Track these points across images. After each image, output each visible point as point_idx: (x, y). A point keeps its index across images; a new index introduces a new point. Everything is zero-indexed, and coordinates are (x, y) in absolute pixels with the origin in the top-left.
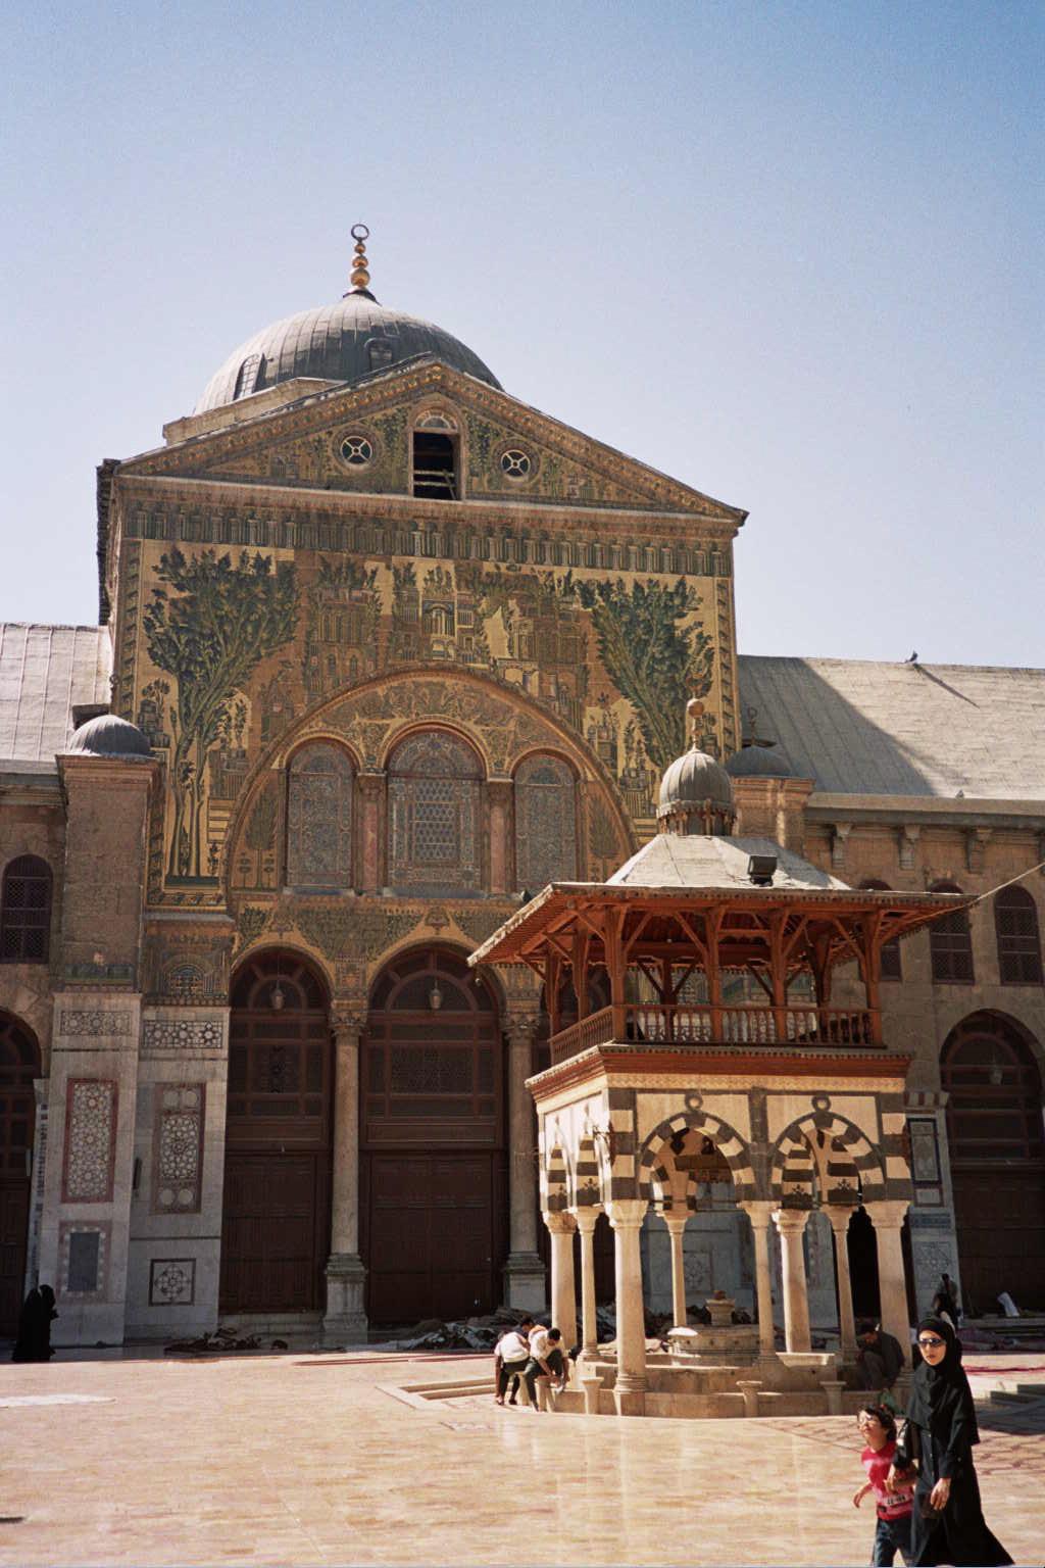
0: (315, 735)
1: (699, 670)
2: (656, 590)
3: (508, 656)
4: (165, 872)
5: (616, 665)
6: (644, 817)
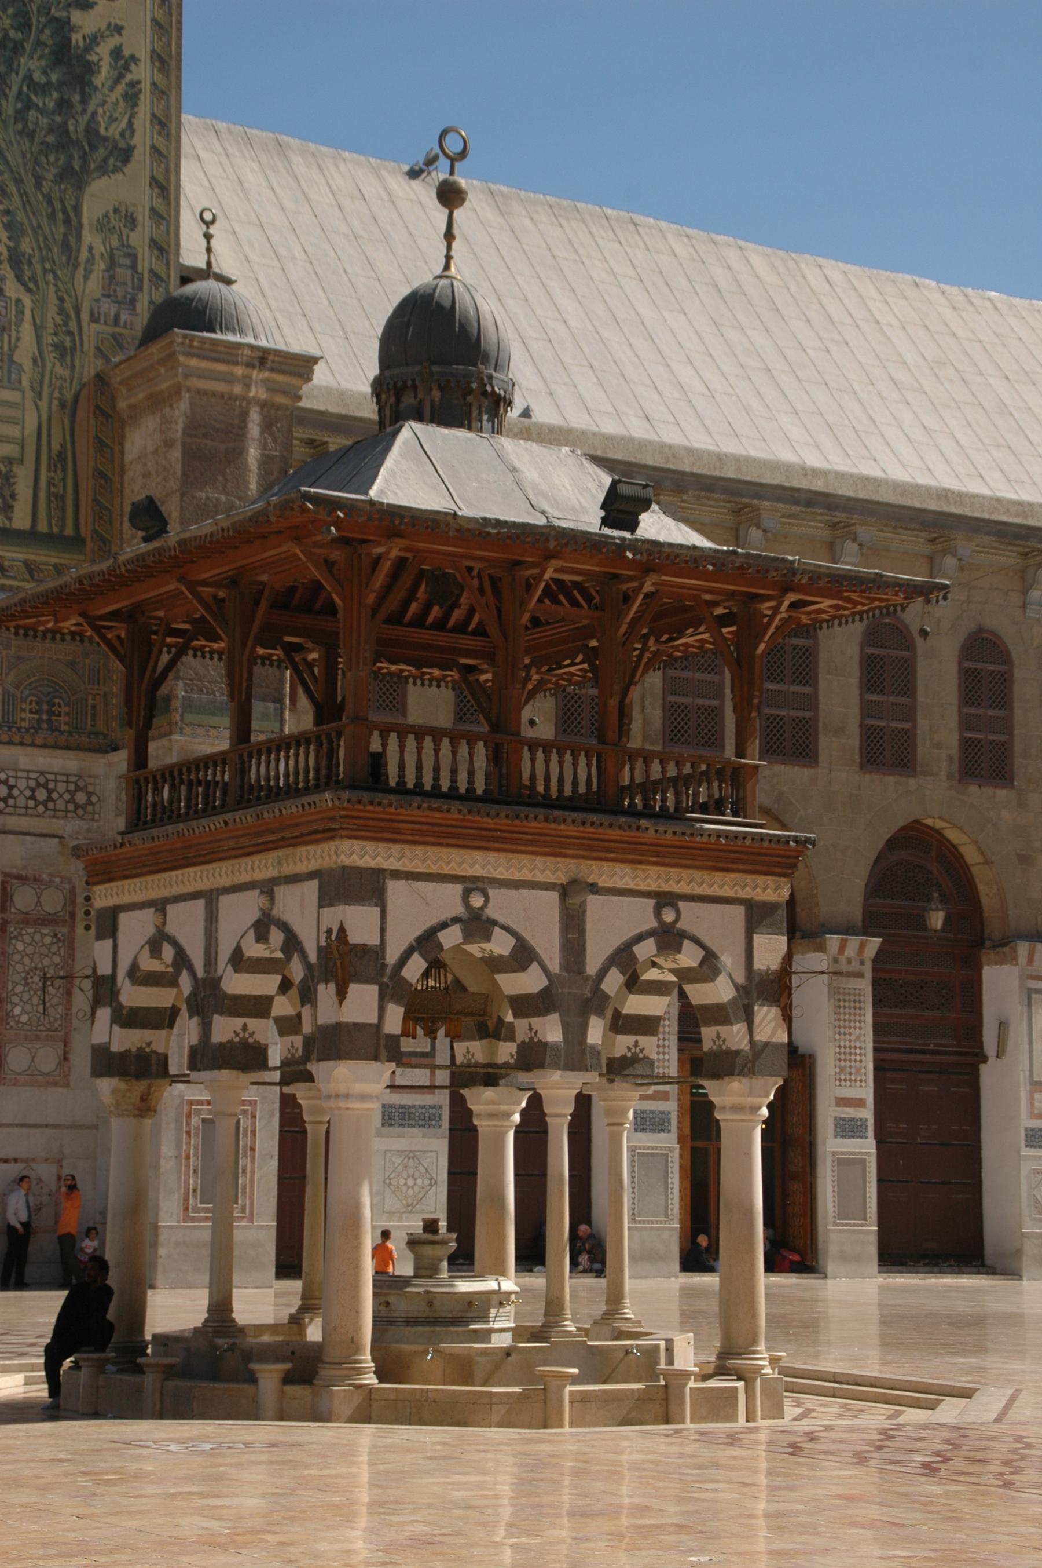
1: (112, 119)
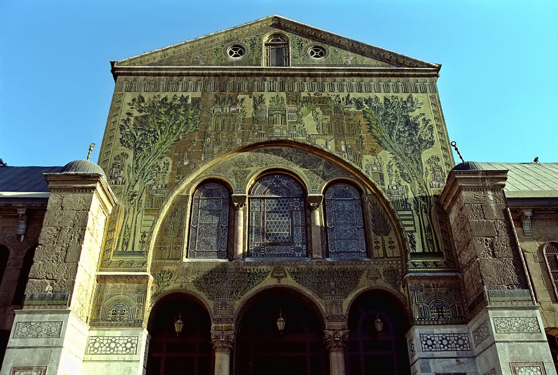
3: (317, 133)
4: (114, 248)
5: (378, 135)
6: (404, 210)
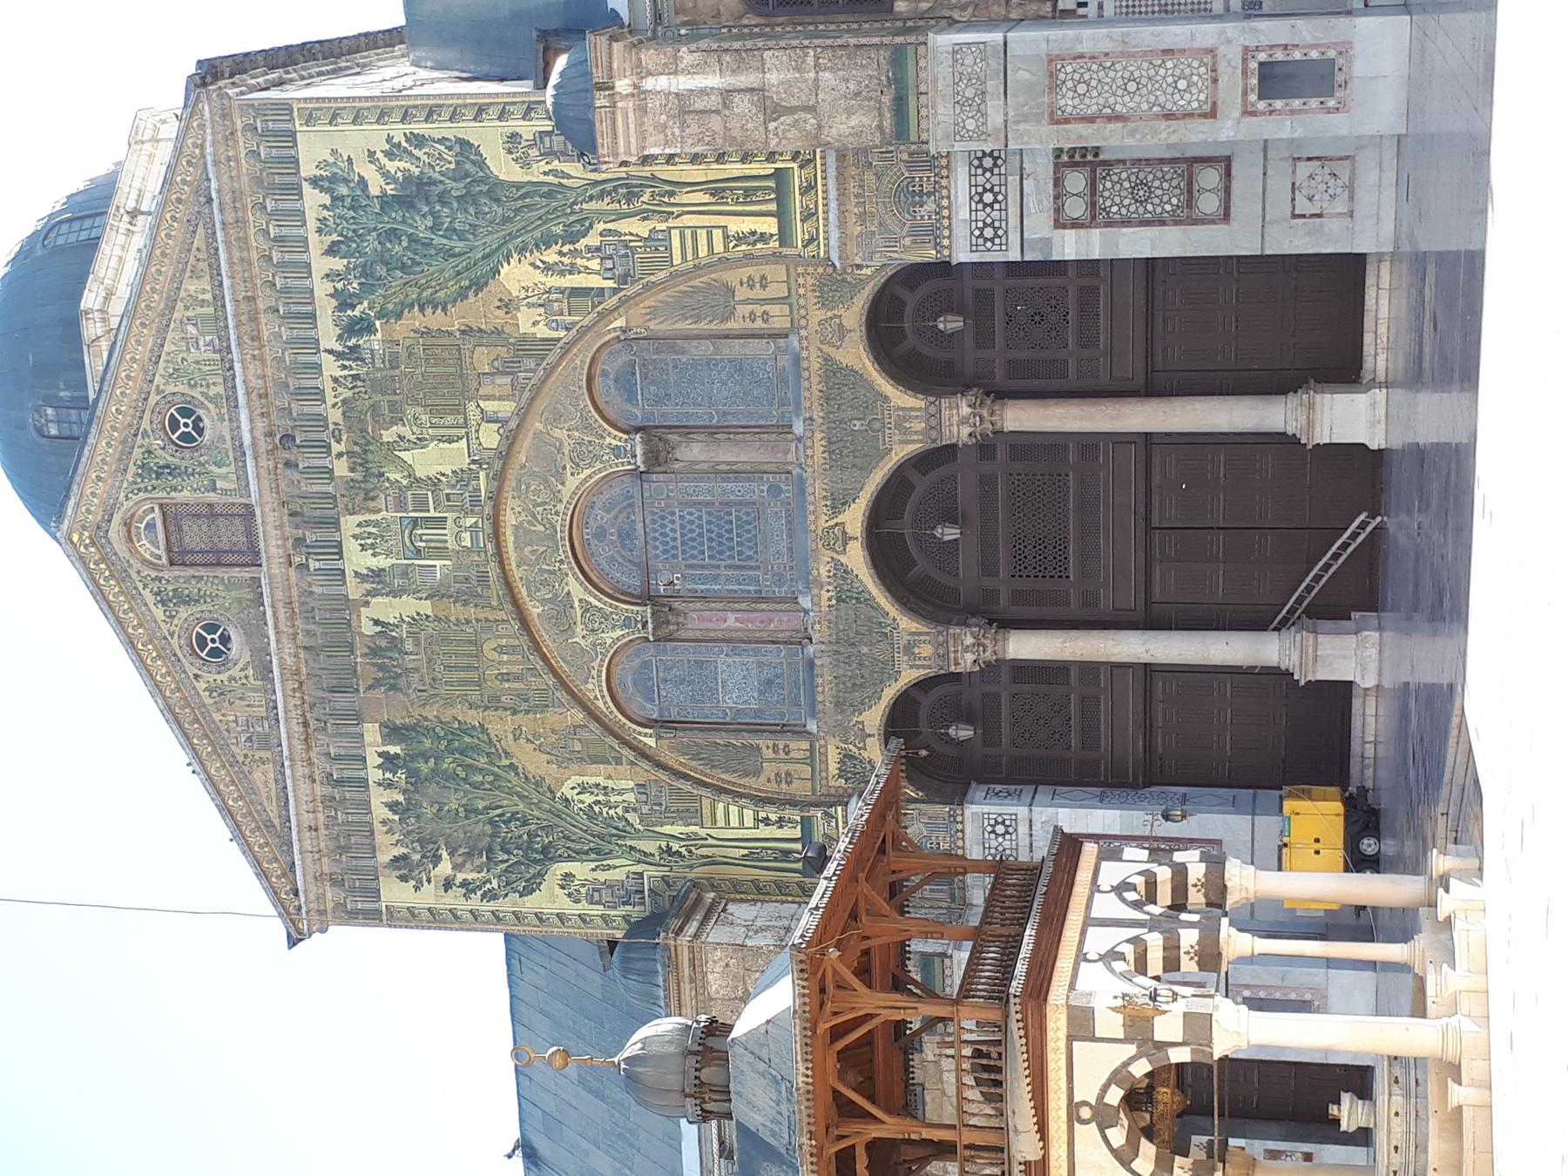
0: (606, 692)
2: (331, 223)
5: (452, 287)
